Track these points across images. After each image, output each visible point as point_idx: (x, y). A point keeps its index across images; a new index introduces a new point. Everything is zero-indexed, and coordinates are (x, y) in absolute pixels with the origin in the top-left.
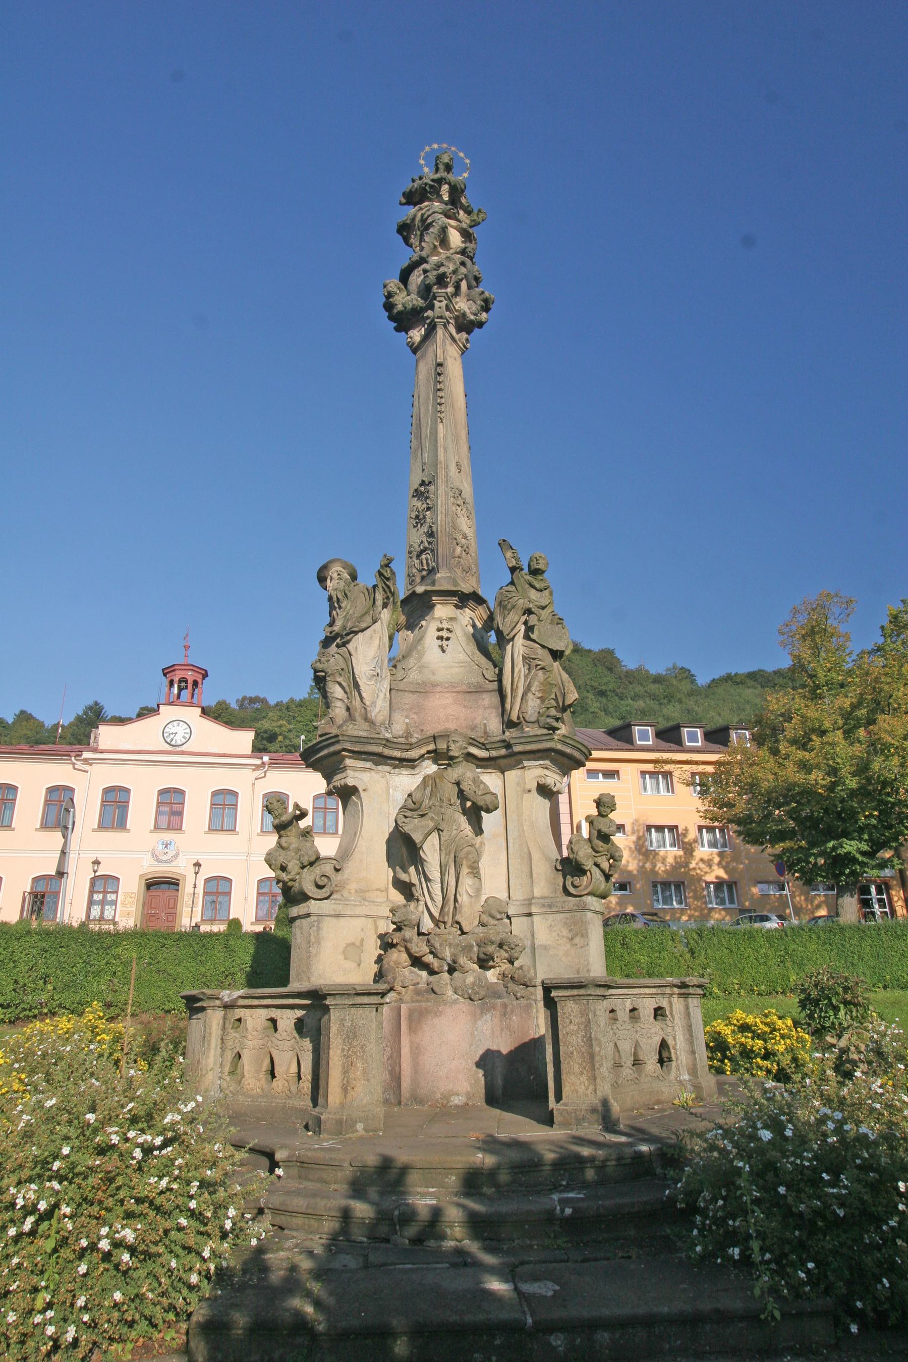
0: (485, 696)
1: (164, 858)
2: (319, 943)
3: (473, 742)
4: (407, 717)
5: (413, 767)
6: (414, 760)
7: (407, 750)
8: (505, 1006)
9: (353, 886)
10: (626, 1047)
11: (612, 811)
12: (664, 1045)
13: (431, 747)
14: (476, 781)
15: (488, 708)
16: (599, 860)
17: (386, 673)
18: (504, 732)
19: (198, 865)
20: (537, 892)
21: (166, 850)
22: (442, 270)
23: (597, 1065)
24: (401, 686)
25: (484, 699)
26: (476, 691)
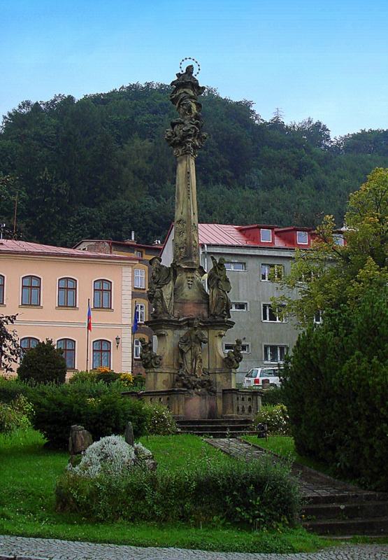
9: (165, 364)
10: (240, 407)
14: (202, 335)
22: (190, 132)
26: (200, 303)
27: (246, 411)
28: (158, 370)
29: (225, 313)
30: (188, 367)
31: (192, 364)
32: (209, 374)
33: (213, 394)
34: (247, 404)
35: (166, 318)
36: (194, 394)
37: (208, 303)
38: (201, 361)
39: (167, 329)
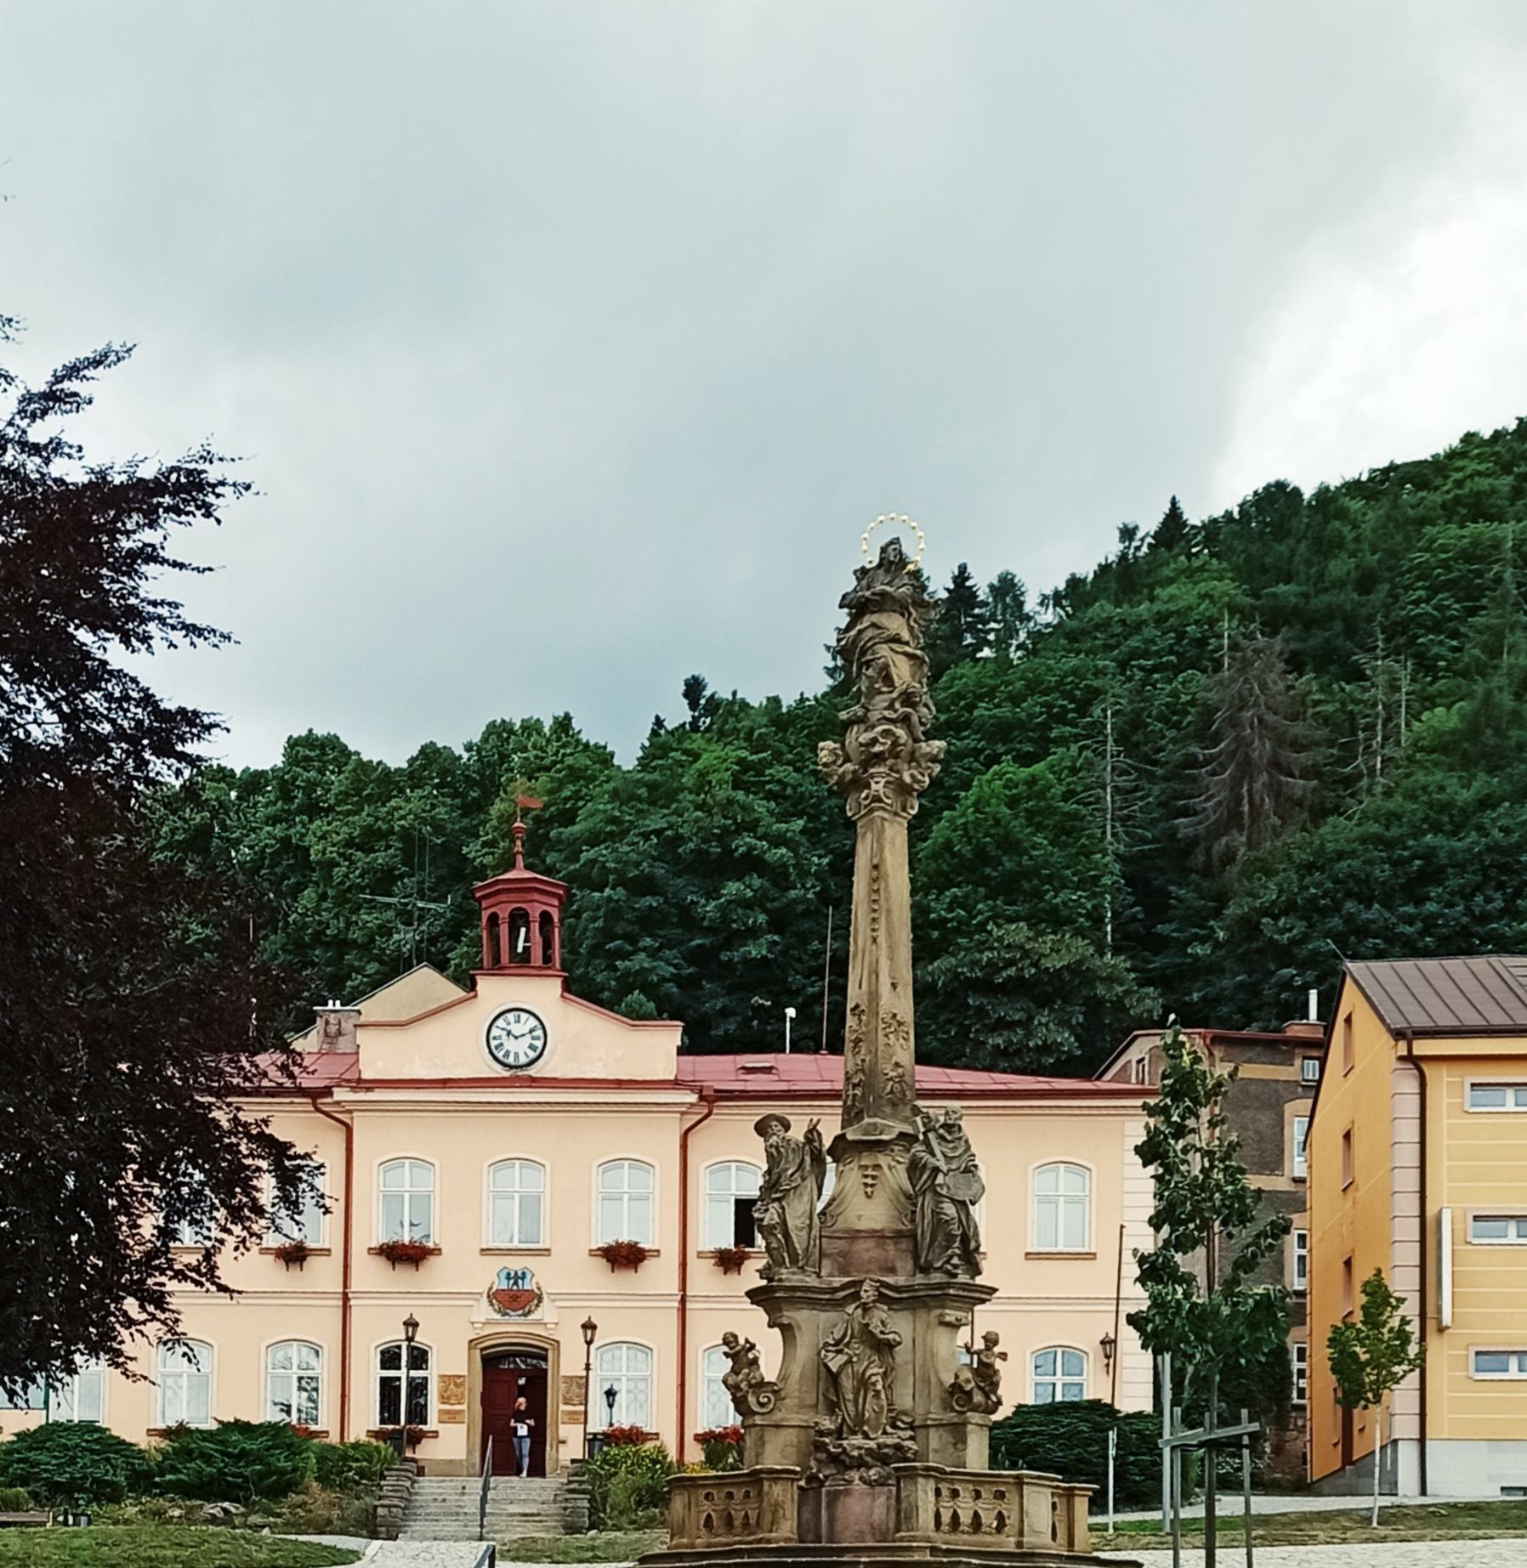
17: (816, 1220)
19: (589, 1326)
31: (856, 1401)
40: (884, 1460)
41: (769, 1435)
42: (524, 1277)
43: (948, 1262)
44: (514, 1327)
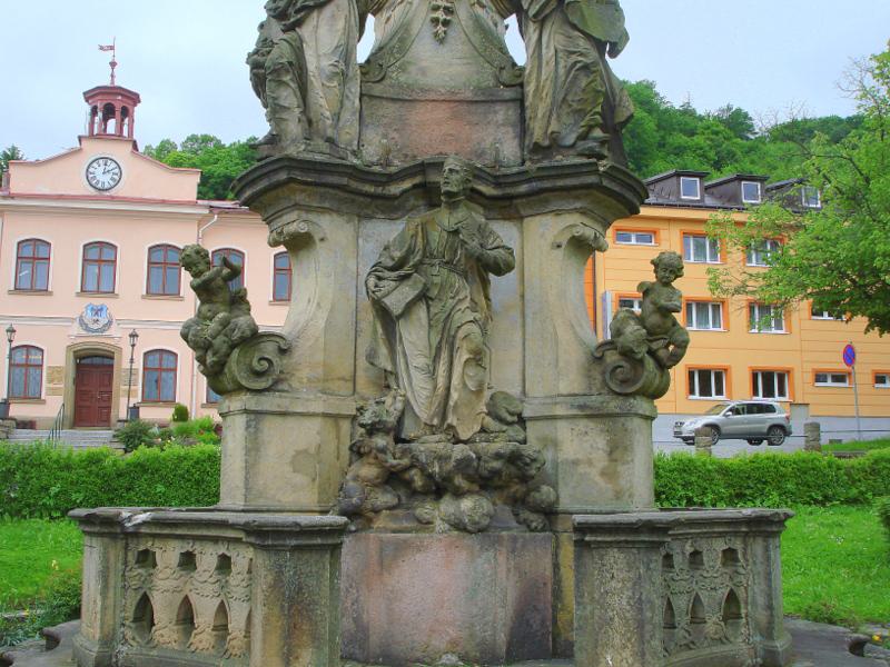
0: (498, 107)
1: (95, 327)
2: (258, 450)
3: (478, 174)
4: (385, 136)
5: (396, 209)
6: (394, 198)
7: (384, 184)
8: (514, 539)
9: (304, 373)
10: (681, 603)
11: (677, 277)
12: (732, 598)
13: (417, 180)
15: (503, 125)
16: (654, 346)
18: (523, 163)
19: (134, 335)
20: (564, 388)
21: (96, 318)
23: (647, 636)
24: (377, 90)
25: (496, 112)
26: (484, 100)
27: (713, 623)
28: (269, 402)
29: (598, 133)
30: (418, 390)
31: (432, 374)
32: (522, 421)
33: (536, 520)
34: (713, 583)
35: (318, 158)
36: (439, 525)
37: (521, 101)
38: (477, 358)
39: (322, 210)
40: (486, 483)
41: (271, 427)
42: (101, 310)
43: (583, 137)
44: (94, 341)
